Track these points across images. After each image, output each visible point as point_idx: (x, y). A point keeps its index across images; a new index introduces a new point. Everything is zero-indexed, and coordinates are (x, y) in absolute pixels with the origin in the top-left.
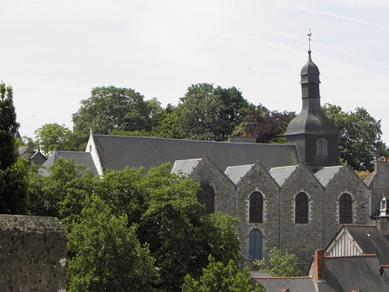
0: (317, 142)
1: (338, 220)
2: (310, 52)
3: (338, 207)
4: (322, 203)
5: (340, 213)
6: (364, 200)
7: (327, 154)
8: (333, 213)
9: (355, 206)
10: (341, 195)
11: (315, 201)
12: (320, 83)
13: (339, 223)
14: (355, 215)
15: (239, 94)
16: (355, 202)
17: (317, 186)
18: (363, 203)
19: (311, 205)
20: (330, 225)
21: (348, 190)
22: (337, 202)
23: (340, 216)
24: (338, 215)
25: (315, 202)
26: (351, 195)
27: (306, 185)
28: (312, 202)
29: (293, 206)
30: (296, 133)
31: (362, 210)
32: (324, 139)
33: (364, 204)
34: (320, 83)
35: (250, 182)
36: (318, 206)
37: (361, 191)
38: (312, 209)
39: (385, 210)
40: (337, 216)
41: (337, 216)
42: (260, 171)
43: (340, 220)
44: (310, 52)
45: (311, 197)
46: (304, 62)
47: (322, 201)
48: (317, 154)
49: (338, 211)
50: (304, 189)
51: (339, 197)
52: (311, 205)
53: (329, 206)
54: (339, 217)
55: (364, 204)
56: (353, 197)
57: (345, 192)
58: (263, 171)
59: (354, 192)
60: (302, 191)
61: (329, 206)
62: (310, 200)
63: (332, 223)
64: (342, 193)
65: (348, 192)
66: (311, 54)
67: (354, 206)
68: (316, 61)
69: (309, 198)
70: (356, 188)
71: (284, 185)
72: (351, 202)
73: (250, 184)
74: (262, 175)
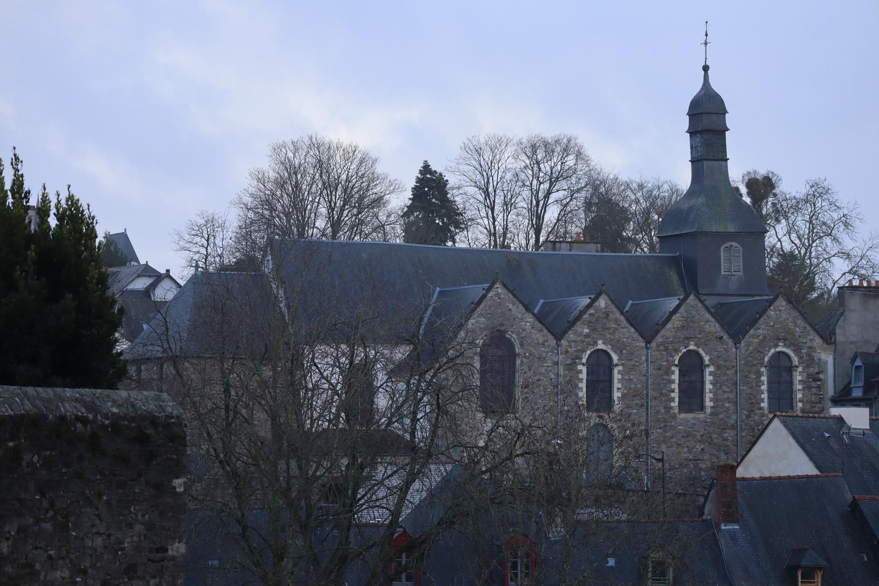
1: (764, 405)
2: (706, 68)
3: (764, 378)
7: (741, 273)
9: (799, 378)
11: (718, 367)
12: (728, 130)
13: (766, 412)
14: (799, 396)
16: (800, 369)
21: (785, 346)
24: (765, 396)
26: (792, 354)
28: (712, 369)
29: (673, 377)
31: (813, 384)
32: (735, 244)
34: (728, 130)
35: (586, 331)
39: (861, 384)
40: (763, 396)
42: (606, 307)
43: (770, 404)
45: (710, 360)
46: (695, 88)
48: (723, 273)
49: (764, 387)
50: (695, 345)
51: (766, 359)
56: (795, 360)
57: (780, 349)
62: (708, 366)
64: (772, 351)
67: (798, 377)
68: (716, 85)
69: (707, 362)
73: (587, 336)
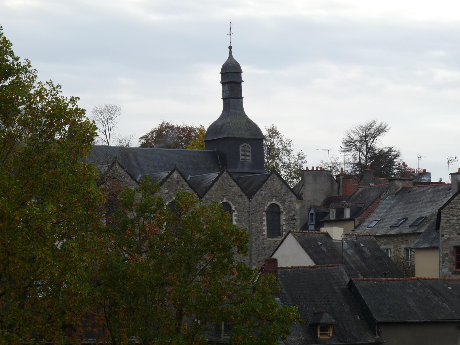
0: (240, 148)
1: (265, 233)
2: (230, 48)
3: (265, 218)
4: (247, 214)
5: (268, 225)
6: (295, 211)
7: (251, 161)
8: (260, 226)
9: (284, 218)
10: (268, 205)
11: (239, 212)
12: (243, 82)
13: (266, 237)
14: (284, 228)
15: (241, 72)
16: (284, 213)
17: (241, 195)
18: (293, 214)
19: (235, 216)
20: (256, 240)
21: (276, 200)
22: (264, 213)
23: (267, 229)
24: (265, 228)
25: (239, 214)
26: (280, 205)
27: (229, 194)
28: (236, 213)
29: (236, 218)
30: (215, 138)
31: (291, 222)
32: (248, 145)
33: (294, 216)
34: (243, 82)
35: (166, 191)
36: (244, 218)
37: (290, 201)
38: (236, 221)
39: (314, 223)
40: (264, 228)
41: (264, 228)
42: (177, 178)
43: (268, 233)
44: (230, 48)
45: (235, 208)
46: (225, 58)
47: (248, 212)
48: (241, 160)
49: (265, 223)
50: (227, 199)
51: (266, 208)
52: (235, 216)
53: (255, 217)
54: (266, 231)
55: (294, 216)
56: (282, 208)
57: (273, 202)
58: (181, 178)
59: (283, 202)
60: (225, 201)
61: (255, 217)
62: (234, 211)
63: (258, 237)
64: (269, 203)
65: (276, 202)
66: (232, 50)
67: (283, 218)
68: (236, 57)
69: (233, 209)
70: (285, 197)
71: (452, 182)
72: (279, 213)
73: (167, 194)
74: (180, 183)
